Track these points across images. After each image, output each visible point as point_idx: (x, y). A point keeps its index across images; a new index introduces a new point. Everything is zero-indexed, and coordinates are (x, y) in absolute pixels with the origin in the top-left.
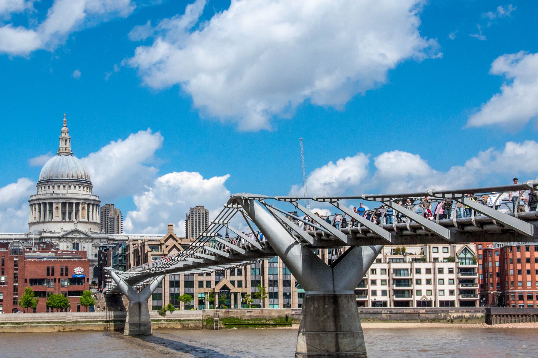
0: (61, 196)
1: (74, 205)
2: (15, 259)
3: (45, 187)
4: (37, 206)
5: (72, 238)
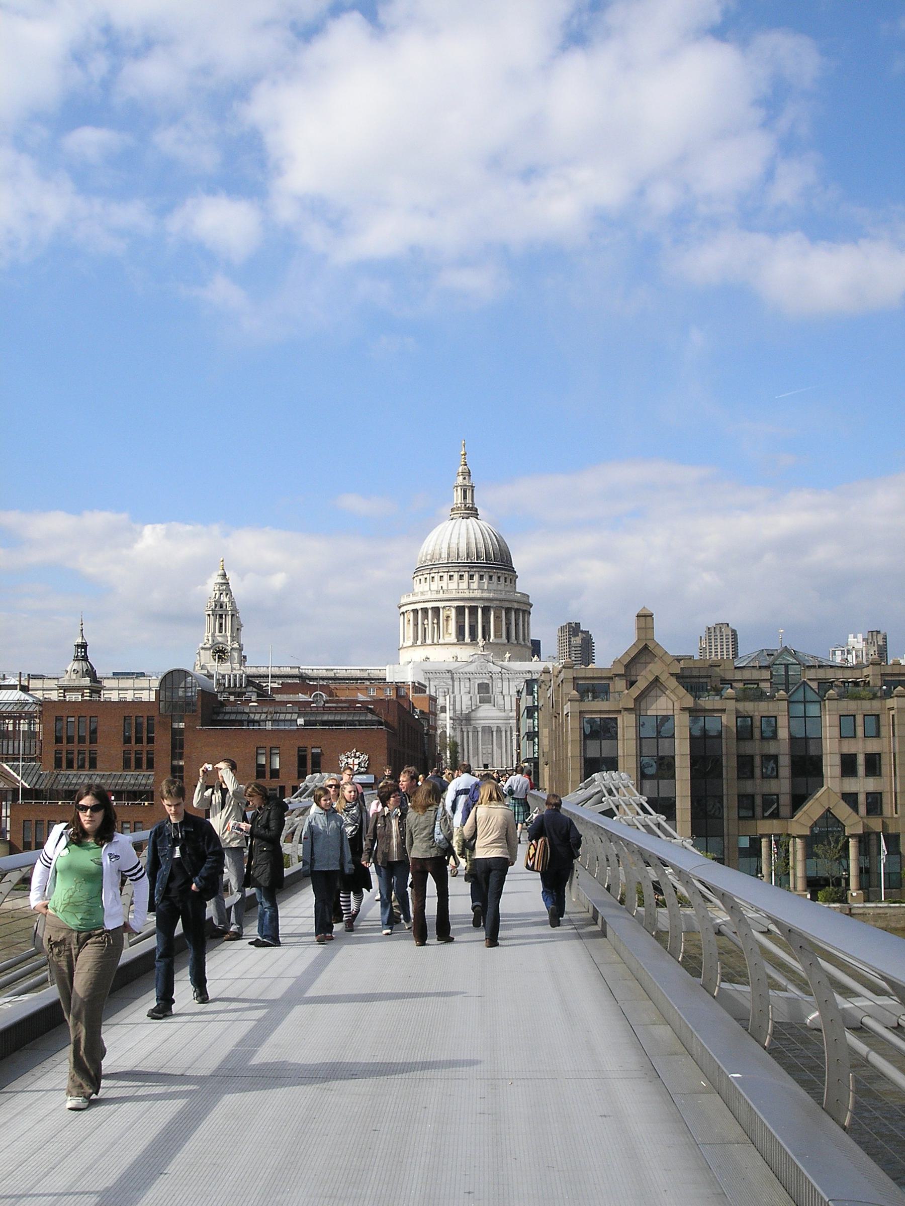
0: (454, 595)
1: (480, 611)
2: (175, 726)
4: (412, 614)
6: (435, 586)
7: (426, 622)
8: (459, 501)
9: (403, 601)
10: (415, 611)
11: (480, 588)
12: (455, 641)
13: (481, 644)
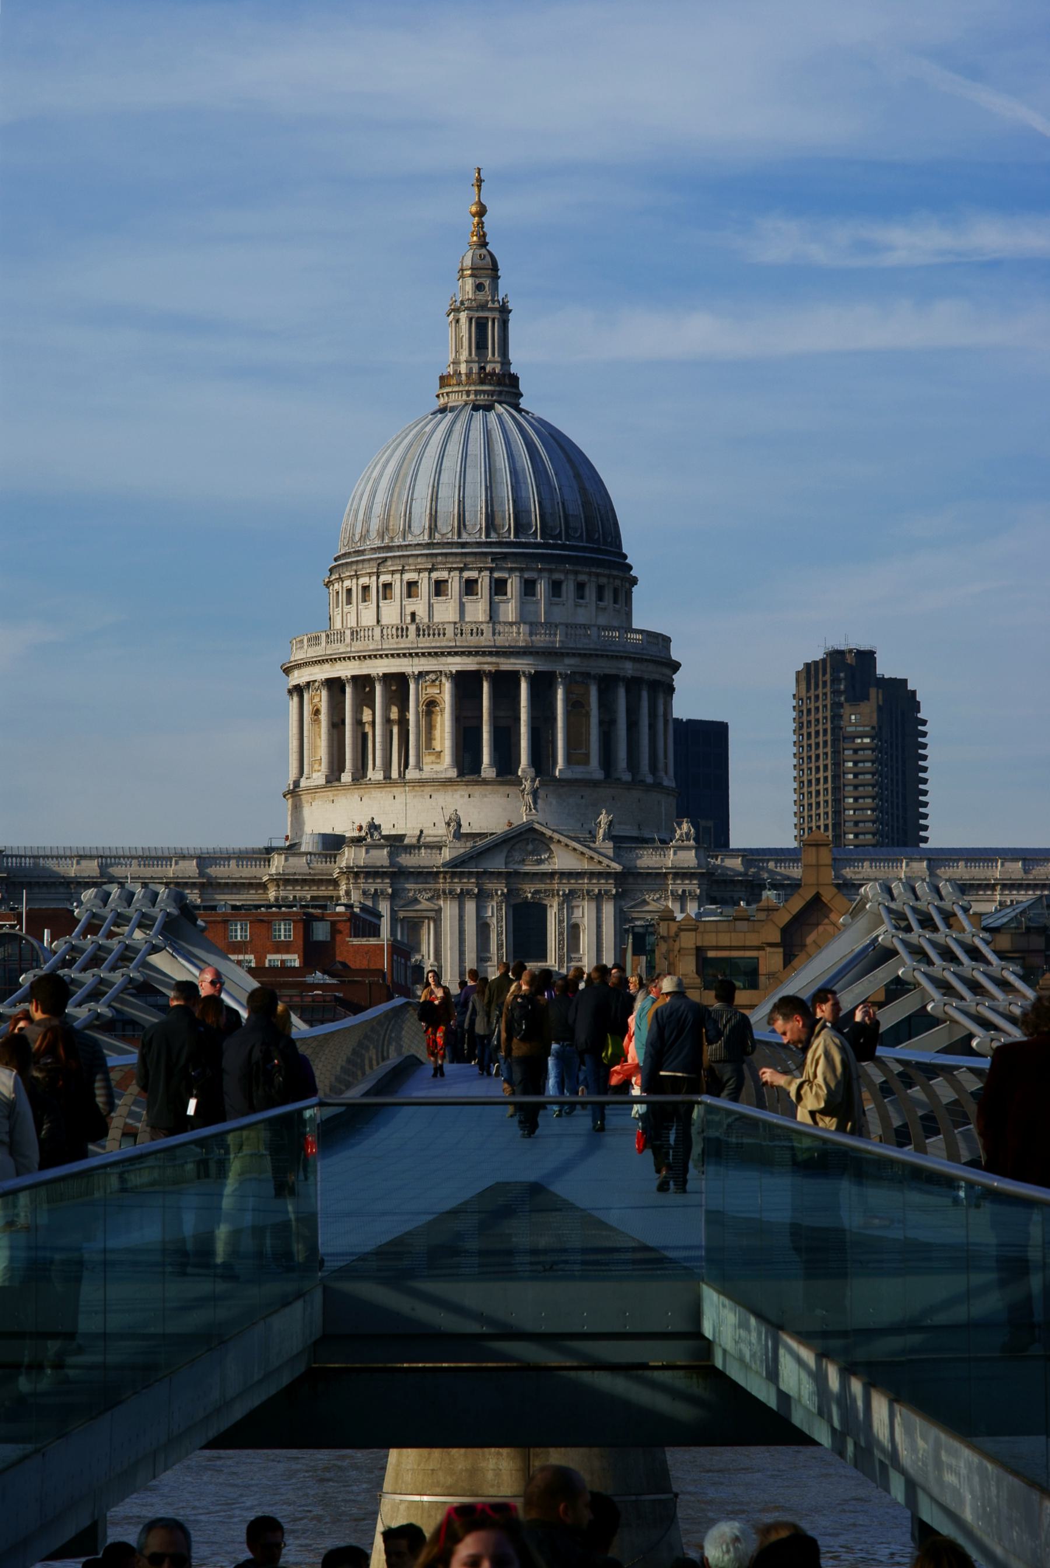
3: (366, 589)
4: (324, 693)
5: (509, 874)
6: (391, 613)
7: (367, 715)
8: (464, 355)
9: (299, 655)
10: (335, 685)
11: (523, 618)
12: (453, 773)
13: (527, 785)
